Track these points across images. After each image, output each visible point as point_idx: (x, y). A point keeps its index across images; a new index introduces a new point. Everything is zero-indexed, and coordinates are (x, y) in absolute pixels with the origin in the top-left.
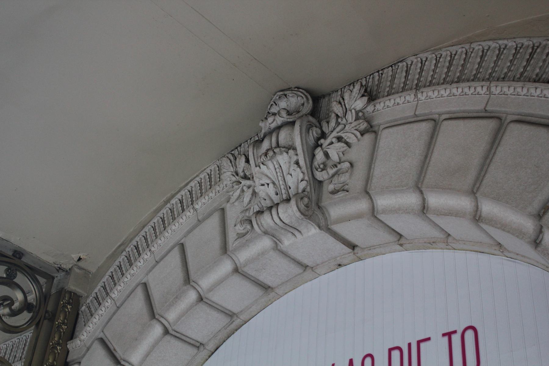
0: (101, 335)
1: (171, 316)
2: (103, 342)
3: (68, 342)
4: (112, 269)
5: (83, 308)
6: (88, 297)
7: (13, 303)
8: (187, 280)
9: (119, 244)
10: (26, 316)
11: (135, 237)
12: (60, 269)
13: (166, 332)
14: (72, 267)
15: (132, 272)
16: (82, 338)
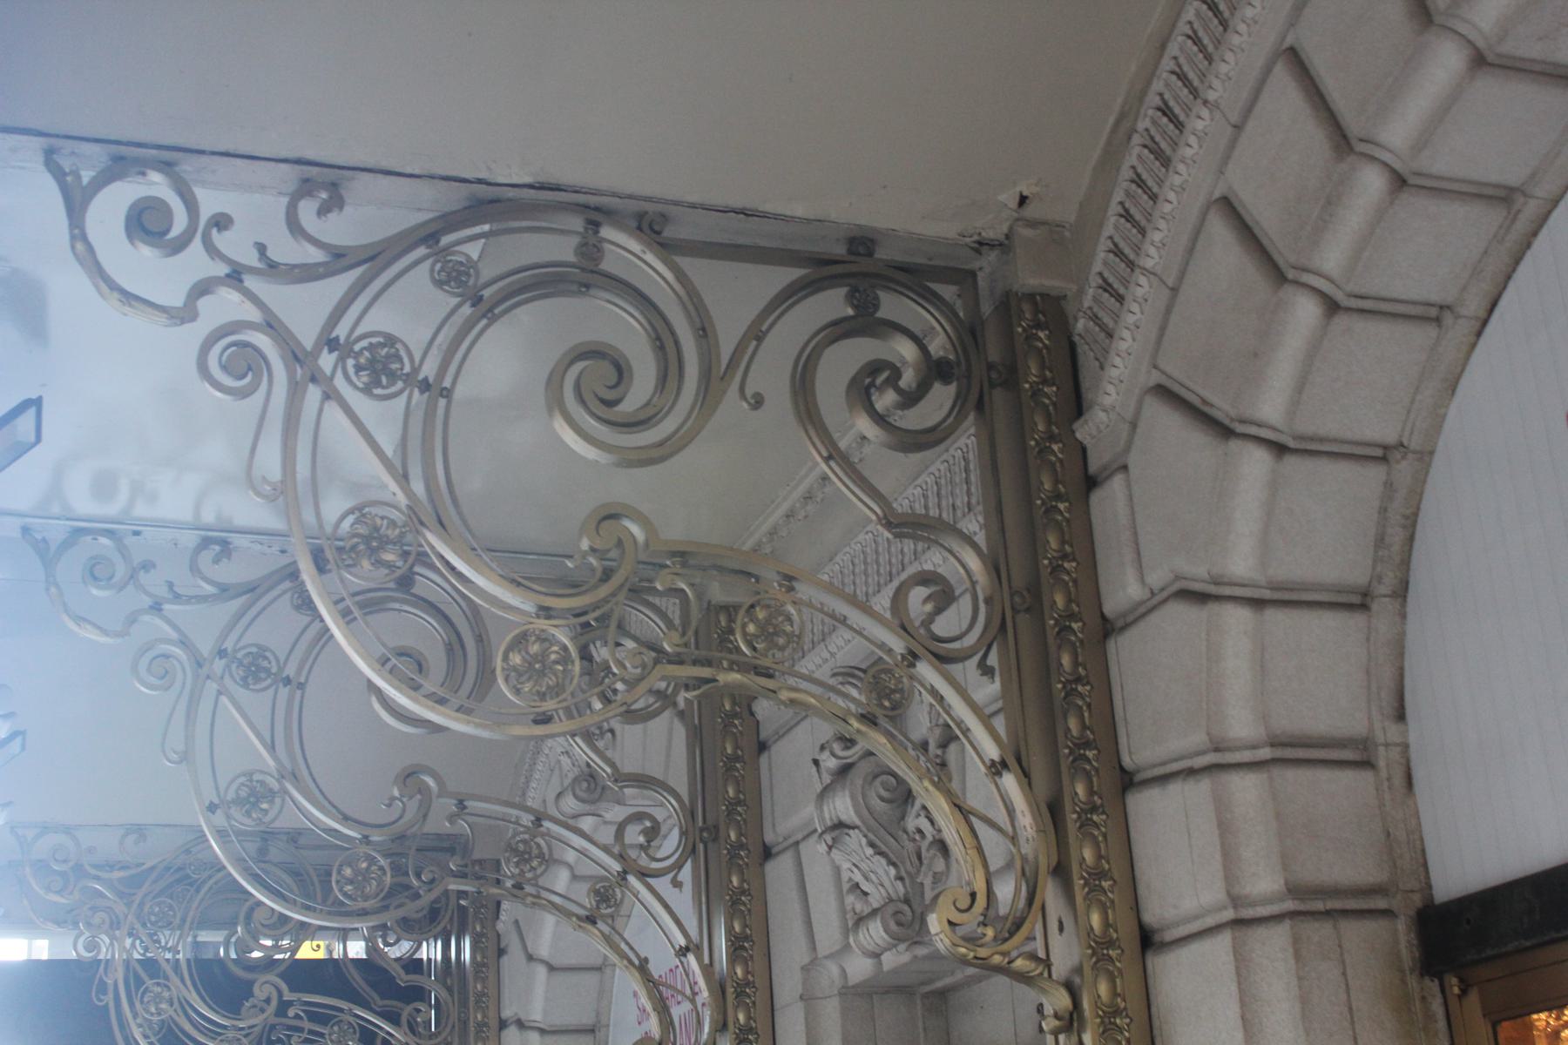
0: (1155, 378)
1: (1332, 257)
2: (1166, 393)
3: (1076, 426)
4: (1118, 196)
5: (1081, 325)
6: (1081, 292)
7: (896, 374)
8: (1343, 142)
9: (1112, 120)
10: (942, 397)
11: (1149, 83)
12: (981, 245)
13: (1332, 307)
14: (1011, 228)
15: (1177, 180)
16: (1107, 401)
